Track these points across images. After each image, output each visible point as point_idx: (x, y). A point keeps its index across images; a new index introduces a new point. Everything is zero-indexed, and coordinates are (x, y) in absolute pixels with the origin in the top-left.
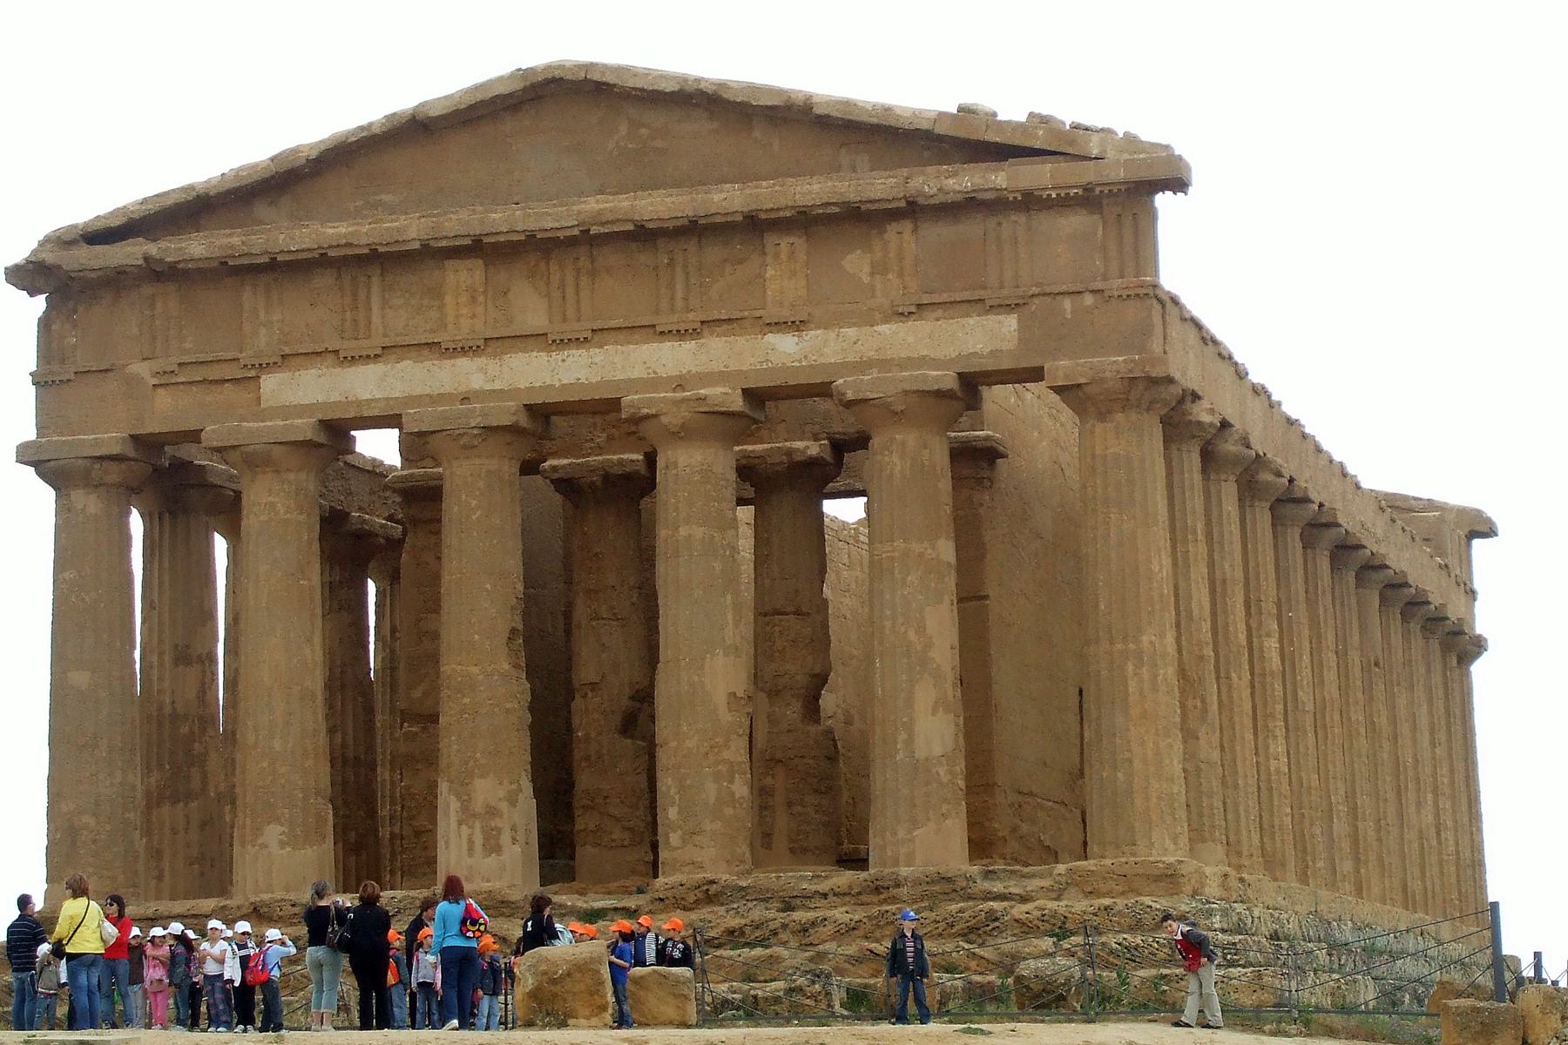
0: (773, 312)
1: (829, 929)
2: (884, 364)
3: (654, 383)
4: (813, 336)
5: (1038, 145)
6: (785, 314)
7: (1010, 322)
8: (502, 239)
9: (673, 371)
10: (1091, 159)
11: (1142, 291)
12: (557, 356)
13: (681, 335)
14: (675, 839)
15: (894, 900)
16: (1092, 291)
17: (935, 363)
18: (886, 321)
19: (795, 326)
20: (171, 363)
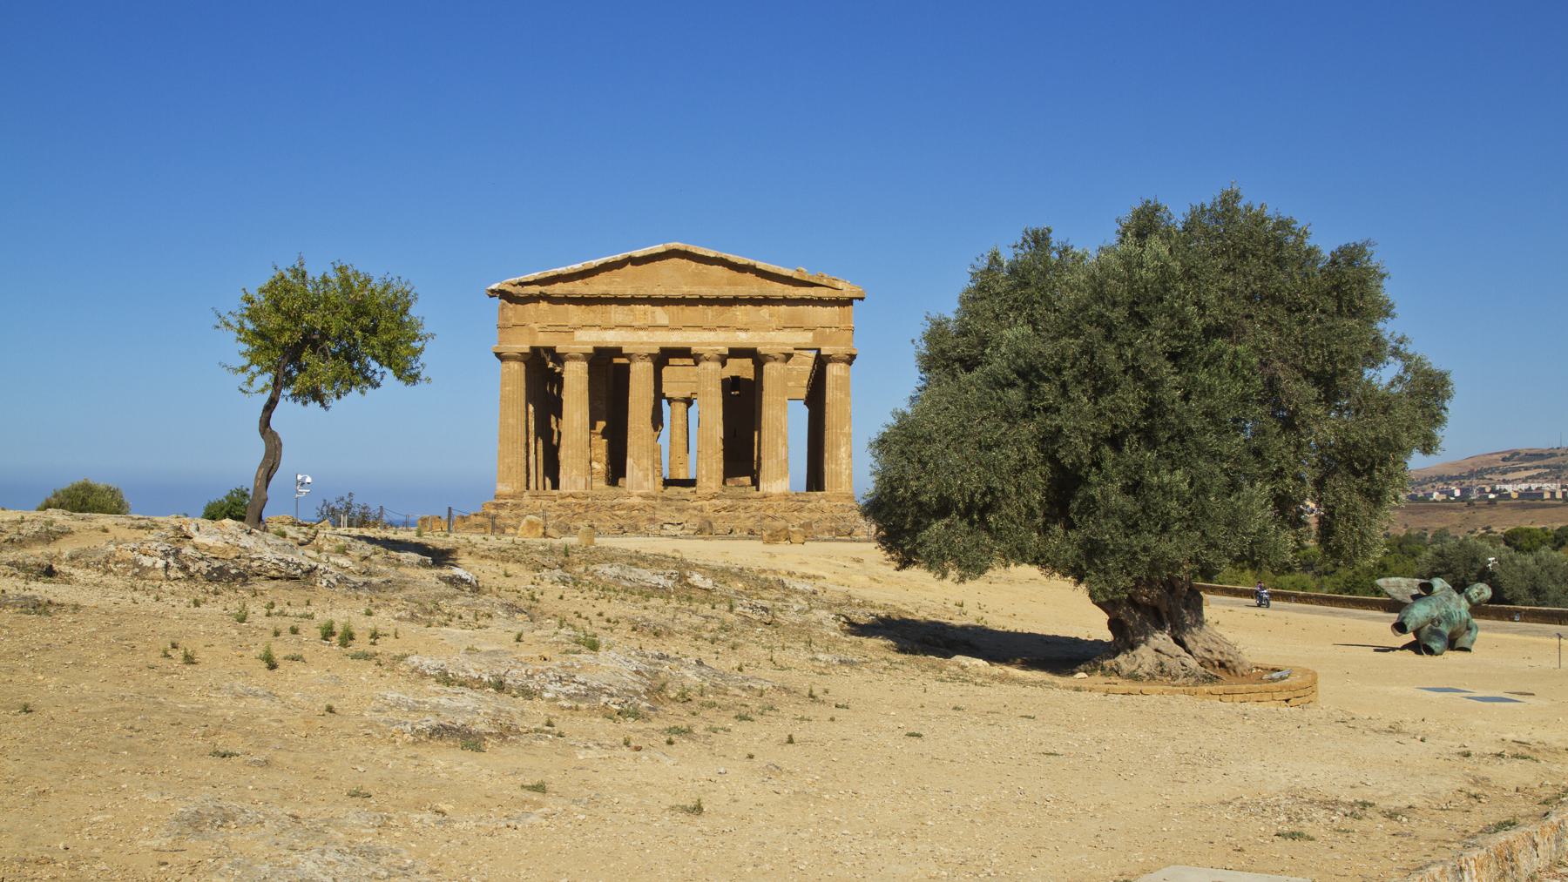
0: (739, 326)
1: (753, 508)
2: (772, 344)
3: (702, 344)
4: (750, 334)
6: (743, 326)
7: (810, 334)
9: (707, 341)
12: (671, 333)
13: (710, 330)
14: (704, 480)
15: (770, 500)
17: (787, 345)
18: (773, 330)
19: (746, 330)
20: (545, 325)
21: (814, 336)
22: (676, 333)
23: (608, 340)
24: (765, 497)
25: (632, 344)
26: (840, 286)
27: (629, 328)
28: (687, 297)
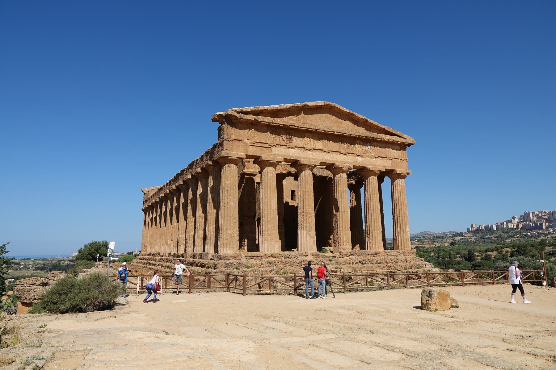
1: (375, 261)
2: (373, 165)
3: (340, 162)
5: (398, 134)
6: (359, 154)
7: (390, 161)
8: (320, 131)
10: (404, 138)
11: (407, 160)
12: (325, 154)
13: (344, 154)
16: (400, 159)
18: (373, 158)
19: (361, 156)
21: (392, 163)
22: (327, 154)
23: (291, 154)
24: (376, 254)
25: (304, 158)
26: (405, 136)
27: (302, 149)
28: (335, 133)
